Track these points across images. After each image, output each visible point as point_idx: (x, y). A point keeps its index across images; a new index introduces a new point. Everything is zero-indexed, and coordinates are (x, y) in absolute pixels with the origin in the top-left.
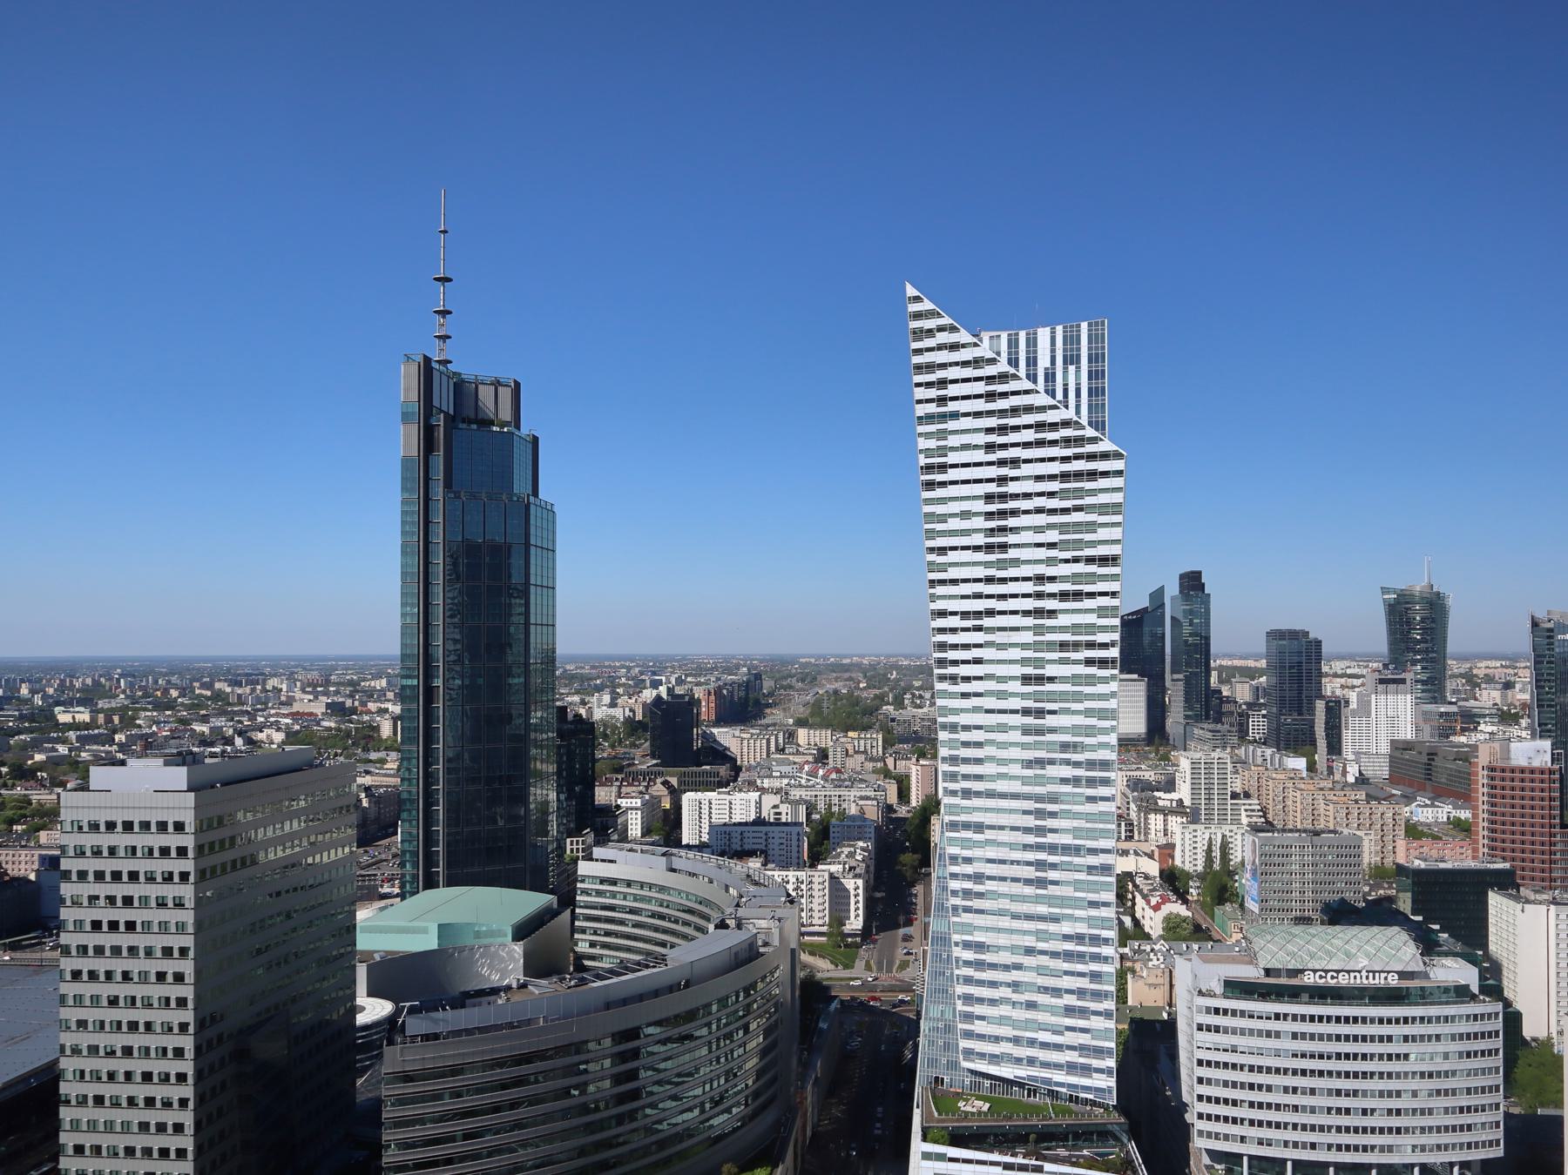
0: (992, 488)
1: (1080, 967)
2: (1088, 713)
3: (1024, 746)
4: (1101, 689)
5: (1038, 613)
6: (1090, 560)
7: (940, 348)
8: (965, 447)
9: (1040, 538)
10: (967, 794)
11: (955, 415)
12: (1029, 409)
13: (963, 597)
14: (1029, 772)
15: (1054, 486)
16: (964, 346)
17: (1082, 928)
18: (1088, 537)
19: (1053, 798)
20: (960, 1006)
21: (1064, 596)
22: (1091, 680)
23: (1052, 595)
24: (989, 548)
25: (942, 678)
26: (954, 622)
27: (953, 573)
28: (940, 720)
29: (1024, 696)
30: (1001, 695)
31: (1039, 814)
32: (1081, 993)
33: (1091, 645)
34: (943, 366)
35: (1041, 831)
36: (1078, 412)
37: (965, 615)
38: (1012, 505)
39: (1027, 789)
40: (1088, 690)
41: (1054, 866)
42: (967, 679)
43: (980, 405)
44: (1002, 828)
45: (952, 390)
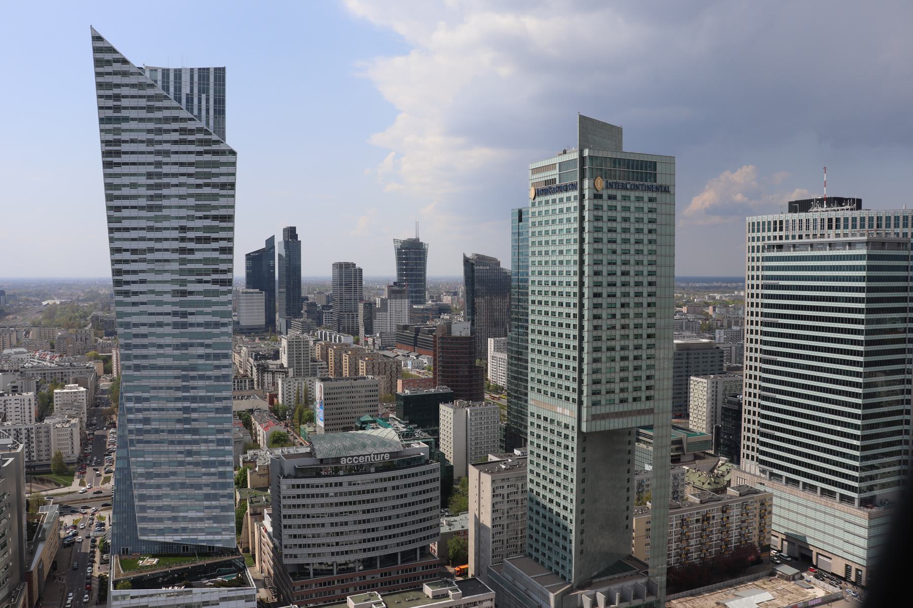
0: (151, 169)
1: (213, 470)
2: (214, 314)
4: (222, 298)
5: (182, 251)
6: (215, 218)
7: (116, 73)
8: (133, 141)
9: (183, 203)
10: (137, 368)
11: (126, 119)
12: (176, 119)
13: (133, 240)
14: (177, 352)
15: (192, 170)
16: (132, 74)
17: (213, 447)
18: (213, 203)
19: (193, 368)
21: (198, 240)
22: (216, 293)
23: (191, 240)
24: (150, 208)
25: (118, 293)
26: (127, 256)
27: (126, 224)
28: (119, 320)
29: (174, 304)
30: (160, 303)
31: (185, 378)
32: (213, 486)
33: (216, 271)
34: (118, 86)
35: (186, 389)
36: (208, 124)
37: (134, 251)
38: (165, 180)
39: (176, 363)
40: (214, 299)
41: (194, 410)
42: (135, 293)
43: (143, 114)
44: (161, 388)
45: (124, 102)
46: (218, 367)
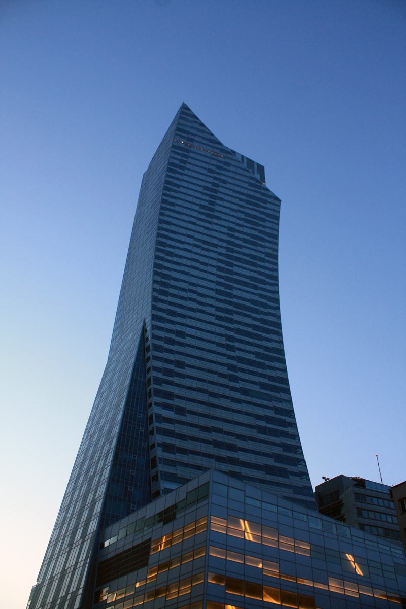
2: (261, 296)
3: (217, 300)
6: (260, 232)
15: (244, 198)
17: (270, 413)
19: (238, 331)
20: (159, 453)
21: (245, 240)
32: (277, 458)
34: (195, 135)
46: (270, 340)
